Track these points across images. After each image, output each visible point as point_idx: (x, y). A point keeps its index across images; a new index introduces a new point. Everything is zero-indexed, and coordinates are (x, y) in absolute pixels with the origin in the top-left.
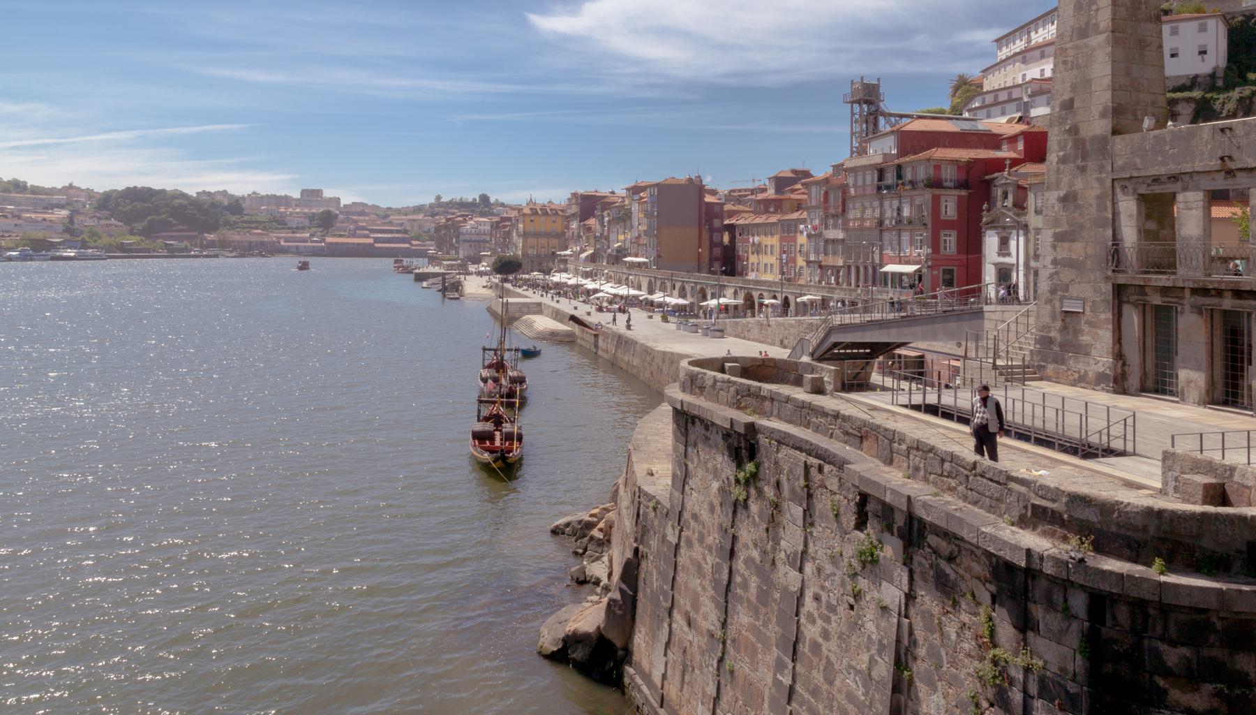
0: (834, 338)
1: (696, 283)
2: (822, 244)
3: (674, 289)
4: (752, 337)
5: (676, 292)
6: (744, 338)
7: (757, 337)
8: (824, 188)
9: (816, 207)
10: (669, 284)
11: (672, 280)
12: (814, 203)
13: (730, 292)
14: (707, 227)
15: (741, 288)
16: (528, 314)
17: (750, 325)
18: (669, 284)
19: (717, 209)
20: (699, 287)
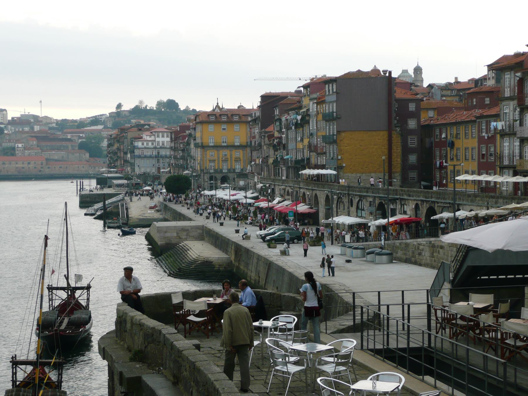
0: (469, 263)
1: (375, 197)
2: (517, 143)
3: (352, 206)
4: (423, 262)
5: (353, 209)
6: (416, 263)
7: (428, 261)
8: (519, 74)
9: (511, 98)
10: (345, 200)
11: (349, 195)
12: (507, 94)
13: (409, 208)
14: (398, 129)
15: (422, 201)
16: (186, 239)
17: (421, 247)
18: (345, 200)
19: (412, 107)
20: (377, 202)
